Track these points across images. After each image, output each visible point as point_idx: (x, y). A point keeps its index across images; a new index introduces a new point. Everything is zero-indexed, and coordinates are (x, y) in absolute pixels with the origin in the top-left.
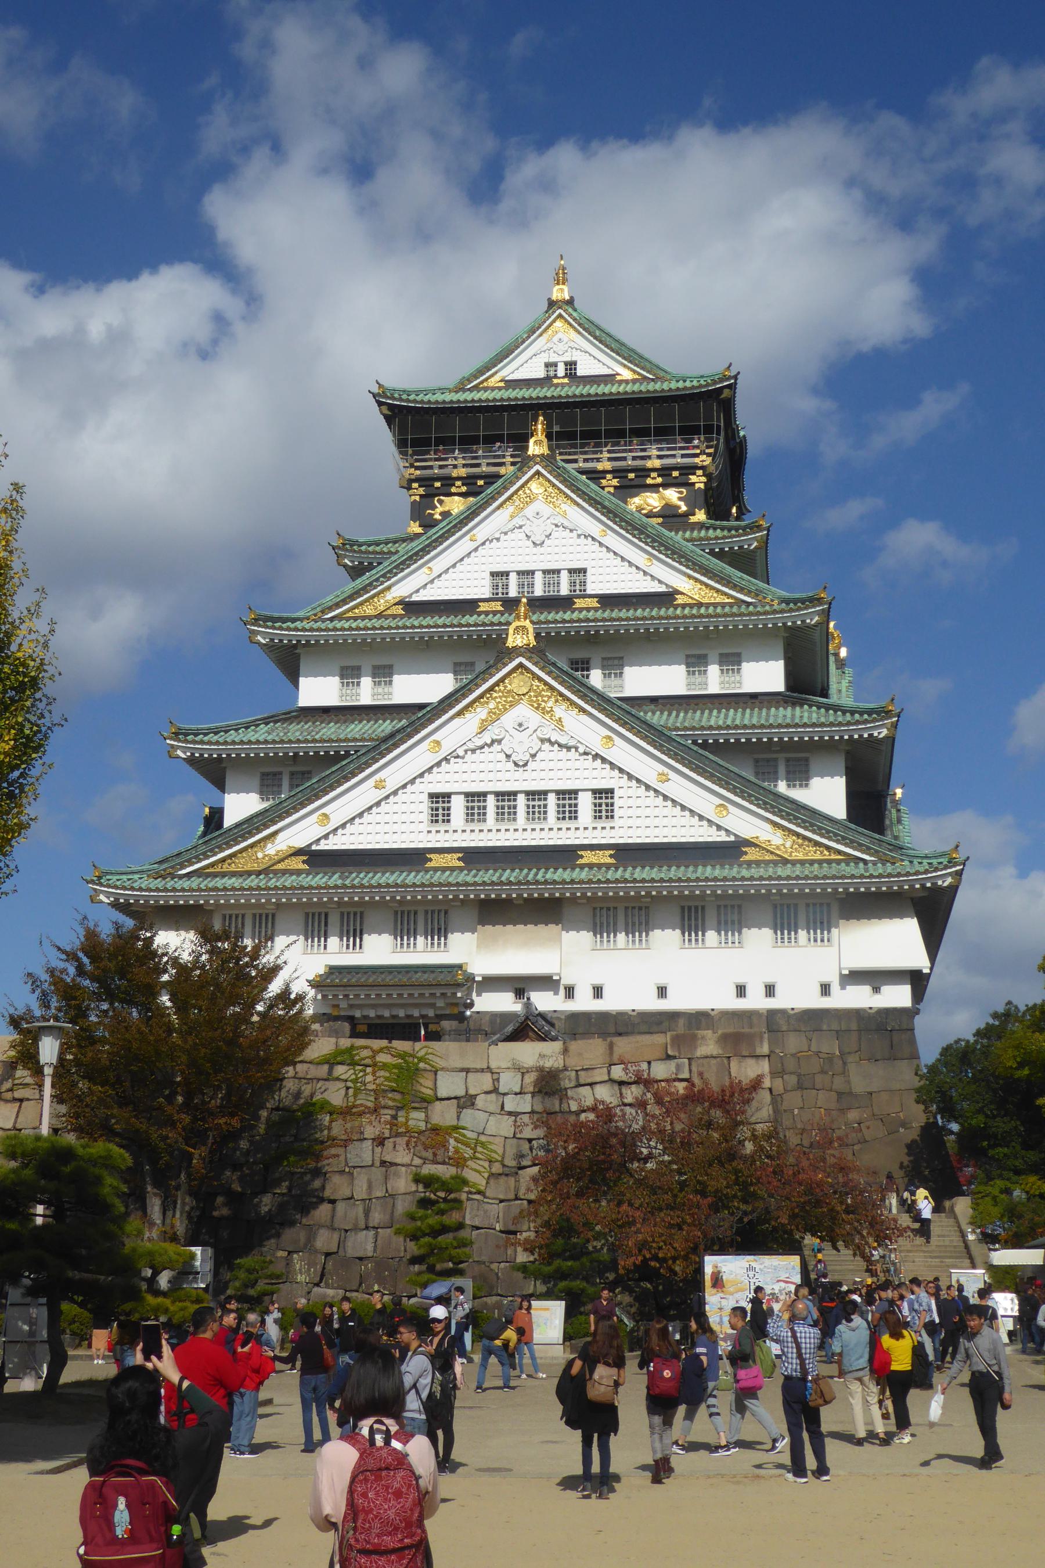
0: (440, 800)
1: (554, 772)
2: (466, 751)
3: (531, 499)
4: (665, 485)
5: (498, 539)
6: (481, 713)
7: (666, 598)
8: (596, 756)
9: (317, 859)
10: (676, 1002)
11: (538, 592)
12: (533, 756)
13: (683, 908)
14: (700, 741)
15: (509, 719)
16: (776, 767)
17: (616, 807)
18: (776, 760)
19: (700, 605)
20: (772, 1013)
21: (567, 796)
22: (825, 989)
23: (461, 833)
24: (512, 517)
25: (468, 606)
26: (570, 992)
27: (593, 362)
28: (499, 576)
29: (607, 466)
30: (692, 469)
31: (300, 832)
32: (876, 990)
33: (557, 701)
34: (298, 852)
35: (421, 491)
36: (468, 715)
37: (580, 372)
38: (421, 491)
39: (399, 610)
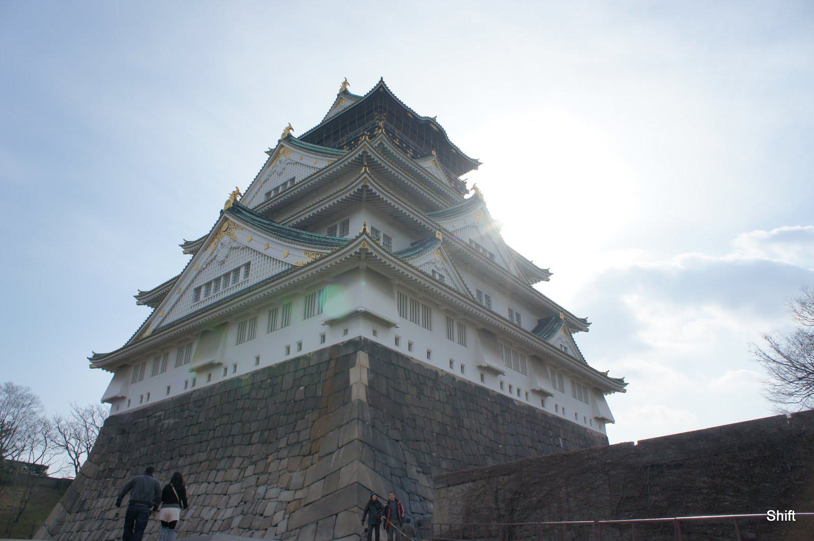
0: (198, 290)
2: (207, 265)
5: (268, 179)
6: (213, 245)
8: (247, 247)
10: (263, 364)
12: (227, 257)
13: (270, 311)
14: (291, 225)
15: (219, 245)
16: (336, 229)
17: (251, 268)
18: (336, 225)
20: (297, 360)
21: (237, 271)
22: (323, 338)
24: (273, 168)
26: (226, 369)
28: (268, 194)
29: (345, 143)
32: (346, 332)
33: (236, 229)
36: (208, 249)
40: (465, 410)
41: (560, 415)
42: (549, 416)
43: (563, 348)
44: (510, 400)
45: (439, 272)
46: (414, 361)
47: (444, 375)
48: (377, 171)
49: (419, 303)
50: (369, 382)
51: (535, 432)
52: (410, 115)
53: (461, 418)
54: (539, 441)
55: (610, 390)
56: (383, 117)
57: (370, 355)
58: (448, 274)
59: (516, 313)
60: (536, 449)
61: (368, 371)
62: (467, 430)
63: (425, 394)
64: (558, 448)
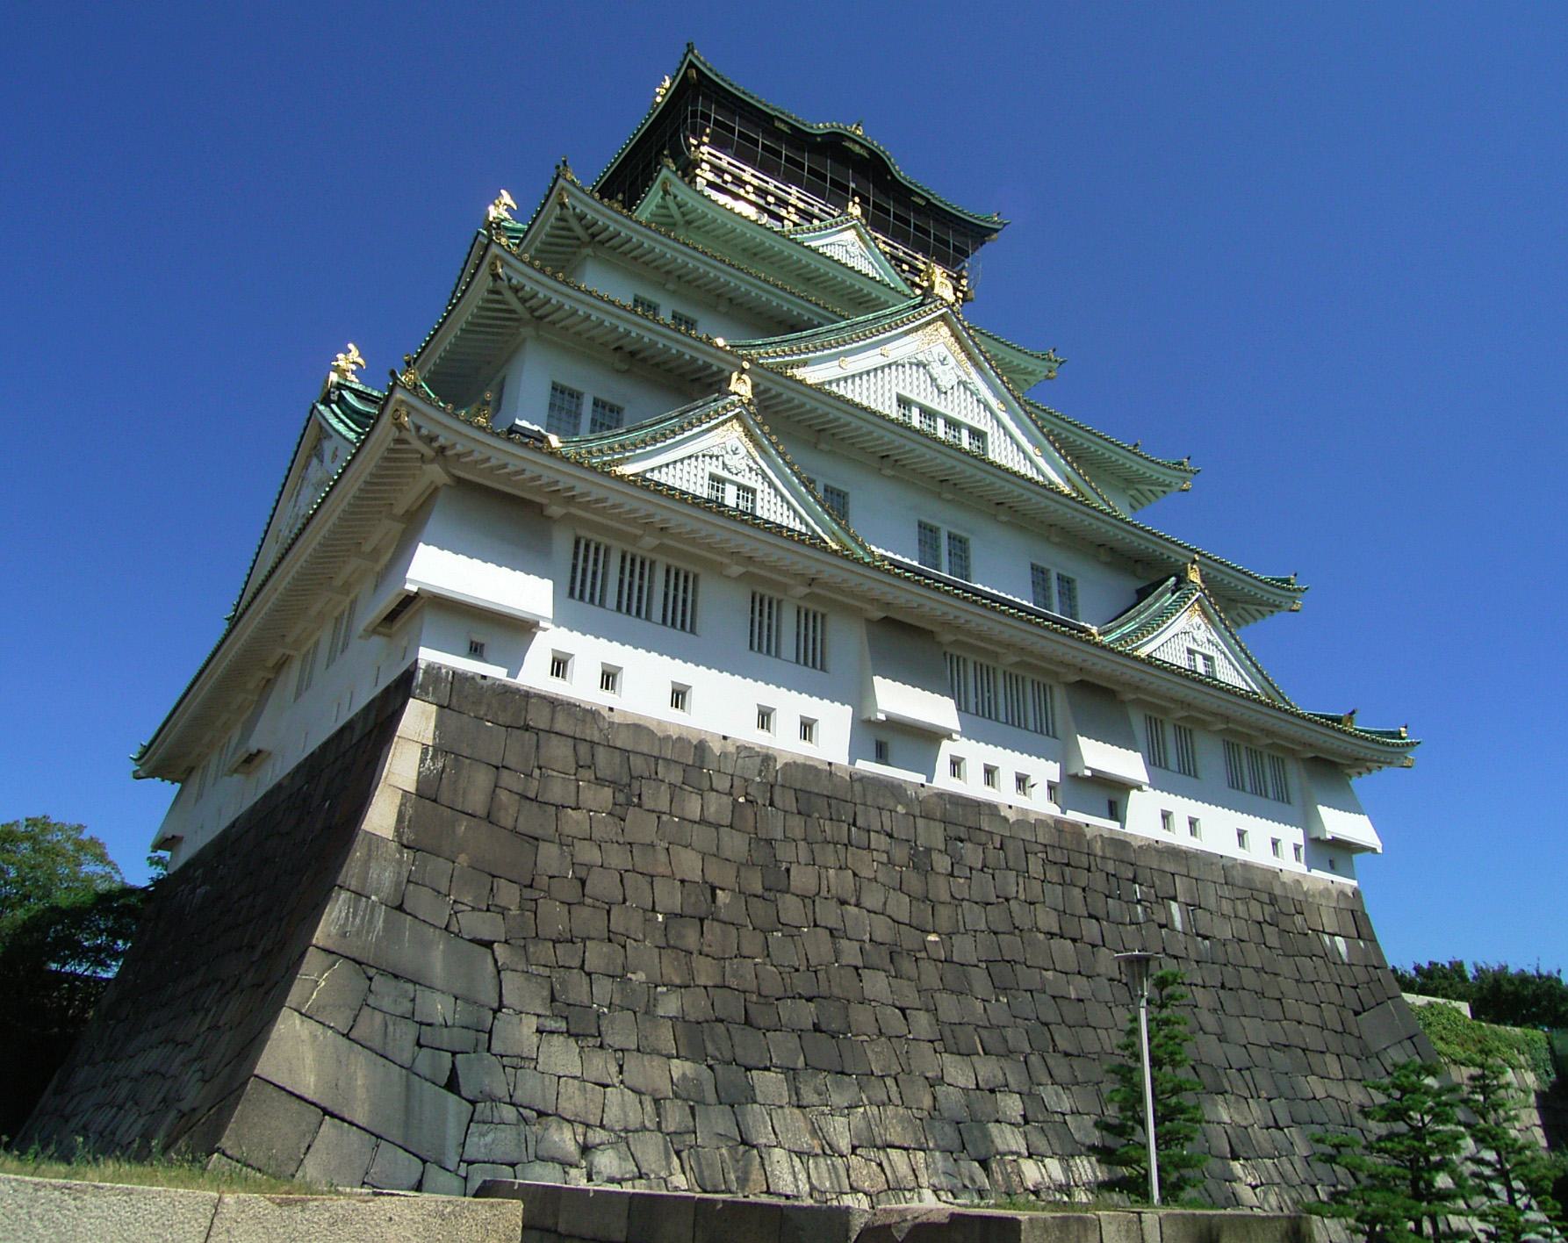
40: (802, 844)
41: (1180, 837)
42: (1135, 844)
43: (1199, 658)
44: (992, 809)
45: (739, 479)
46: (617, 719)
47: (732, 749)
48: (635, 258)
49: (652, 563)
50: (422, 780)
51: (1077, 892)
52: (782, 126)
53: (784, 866)
54: (1091, 916)
55: (1360, 763)
56: (706, 139)
57: (441, 706)
58: (771, 484)
59: (1060, 577)
60: (1074, 940)
61: (425, 751)
62: (803, 897)
63: (648, 803)
64: (1164, 931)
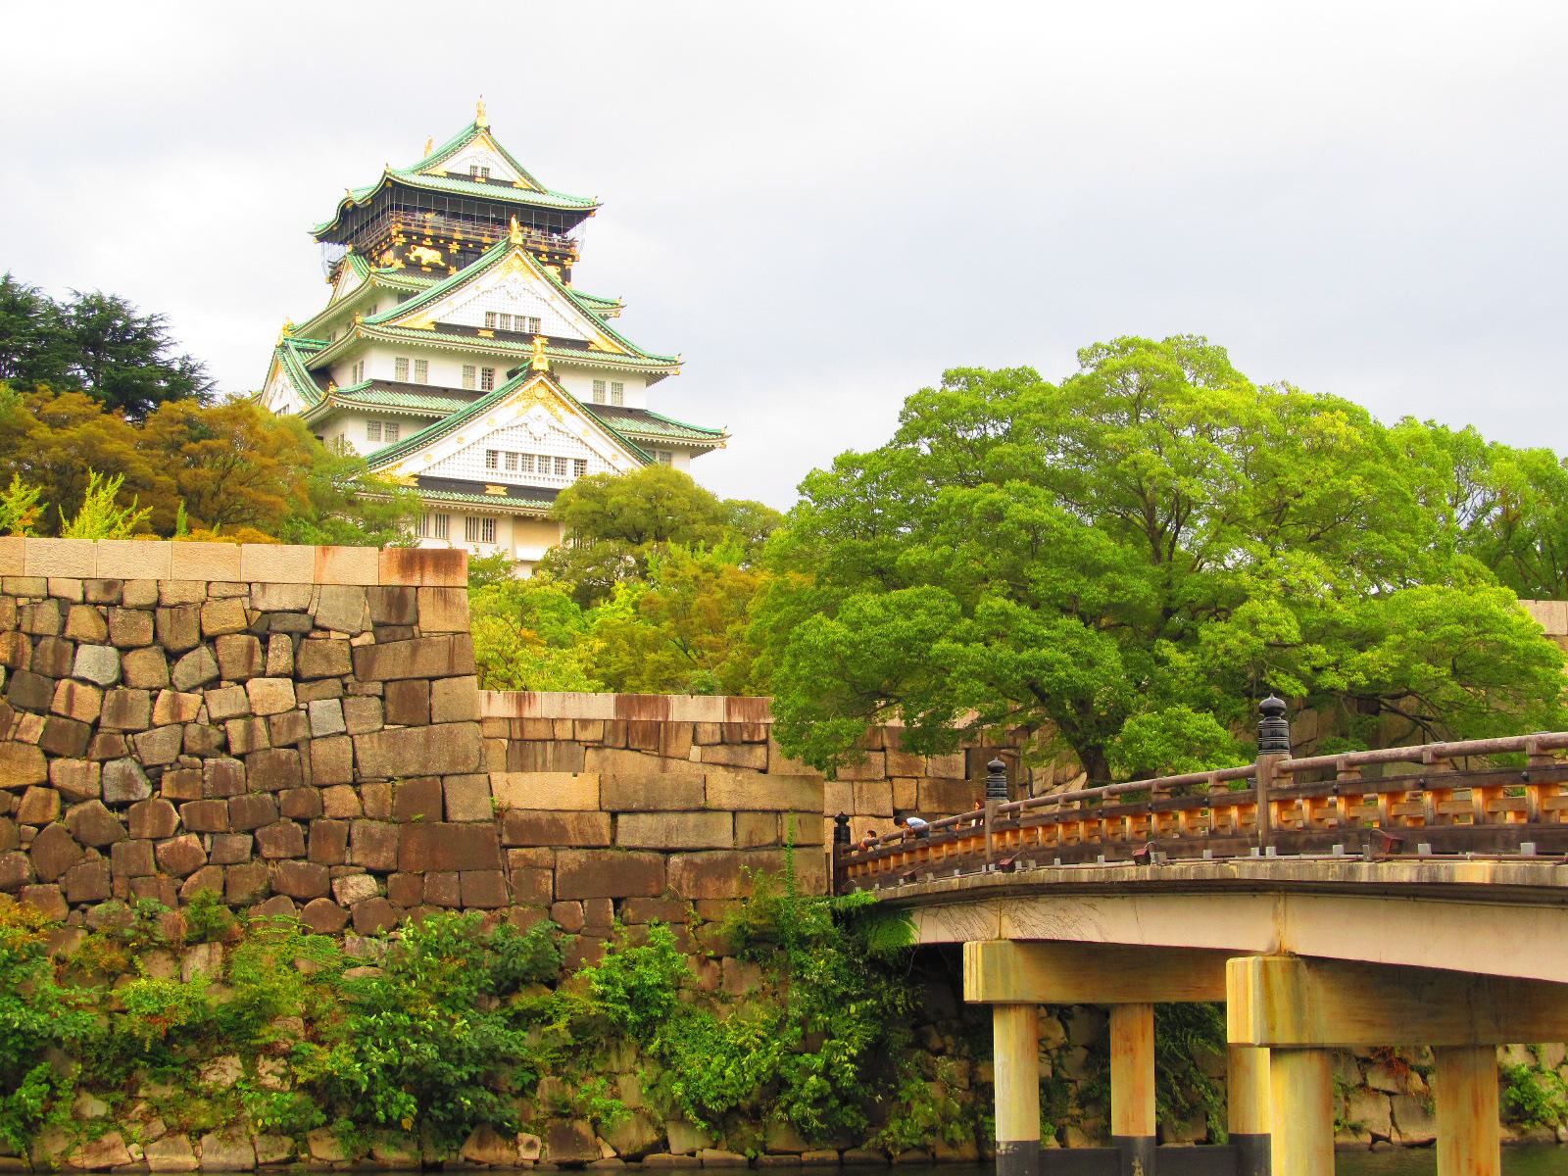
0: (493, 453)
1: (556, 447)
3: (510, 268)
4: (549, 263)
7: (583, 345)
9: (425, 482)
11: (513, 329)
19: (601, 351)
23: (503, 475)
25: (472, 331)
27: (501, 171)
30: (564, 256)
31: (415, 464)
34: (415, 476)
35: (404, 240)
37: (492, 176)
38: (404, 240)
39: (432, 327)
